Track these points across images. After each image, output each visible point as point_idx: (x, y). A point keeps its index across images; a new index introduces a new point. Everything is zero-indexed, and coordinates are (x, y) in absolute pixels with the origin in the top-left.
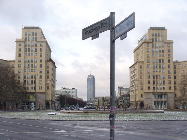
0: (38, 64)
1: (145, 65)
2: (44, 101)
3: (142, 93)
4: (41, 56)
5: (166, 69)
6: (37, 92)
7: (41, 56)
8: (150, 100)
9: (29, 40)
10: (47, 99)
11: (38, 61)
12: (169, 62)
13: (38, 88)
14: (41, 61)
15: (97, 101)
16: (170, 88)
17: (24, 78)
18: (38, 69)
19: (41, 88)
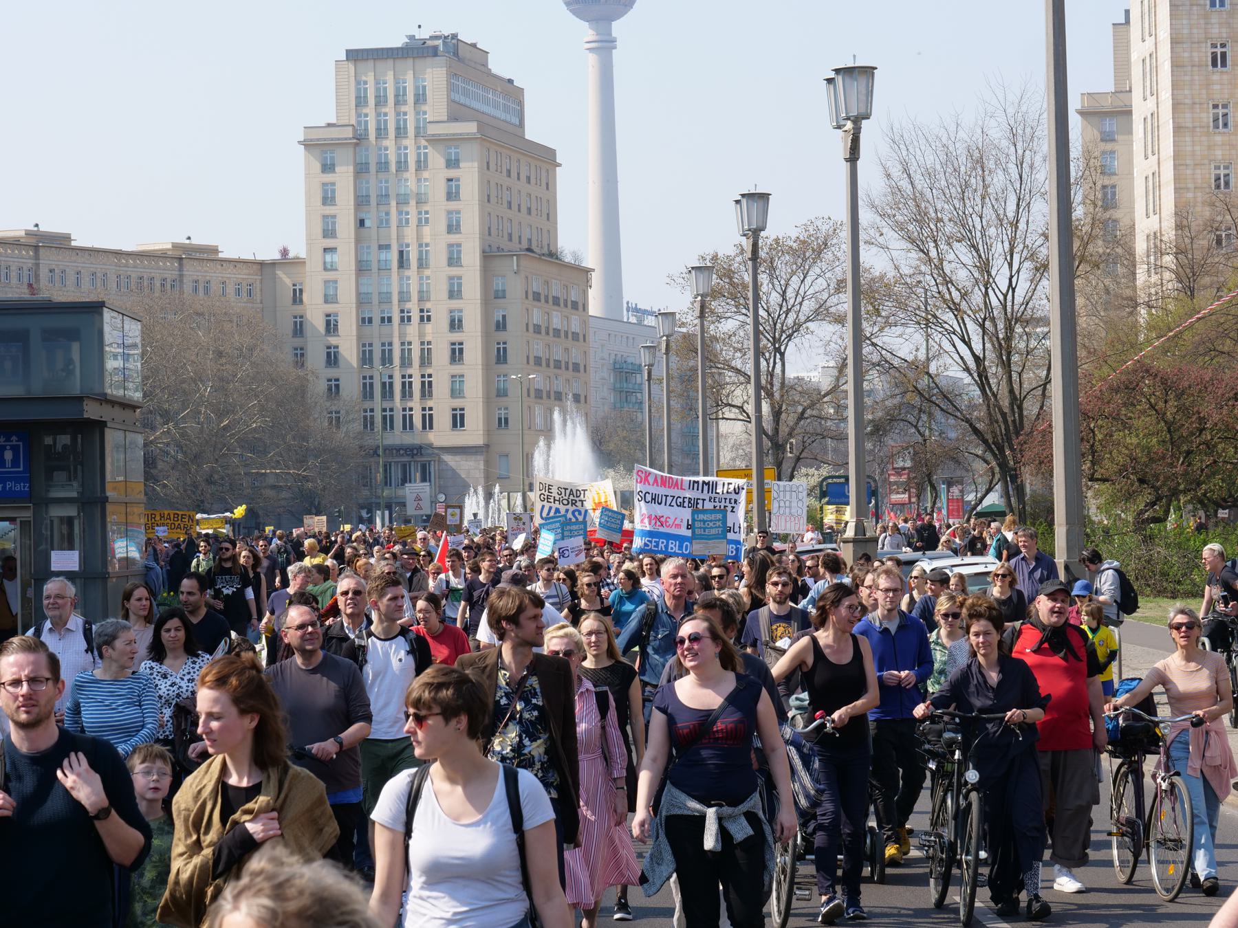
9: (381, 132)
11: (438, 257)
13: (442, 419)
14: (454, 259)
19: (458, 420)
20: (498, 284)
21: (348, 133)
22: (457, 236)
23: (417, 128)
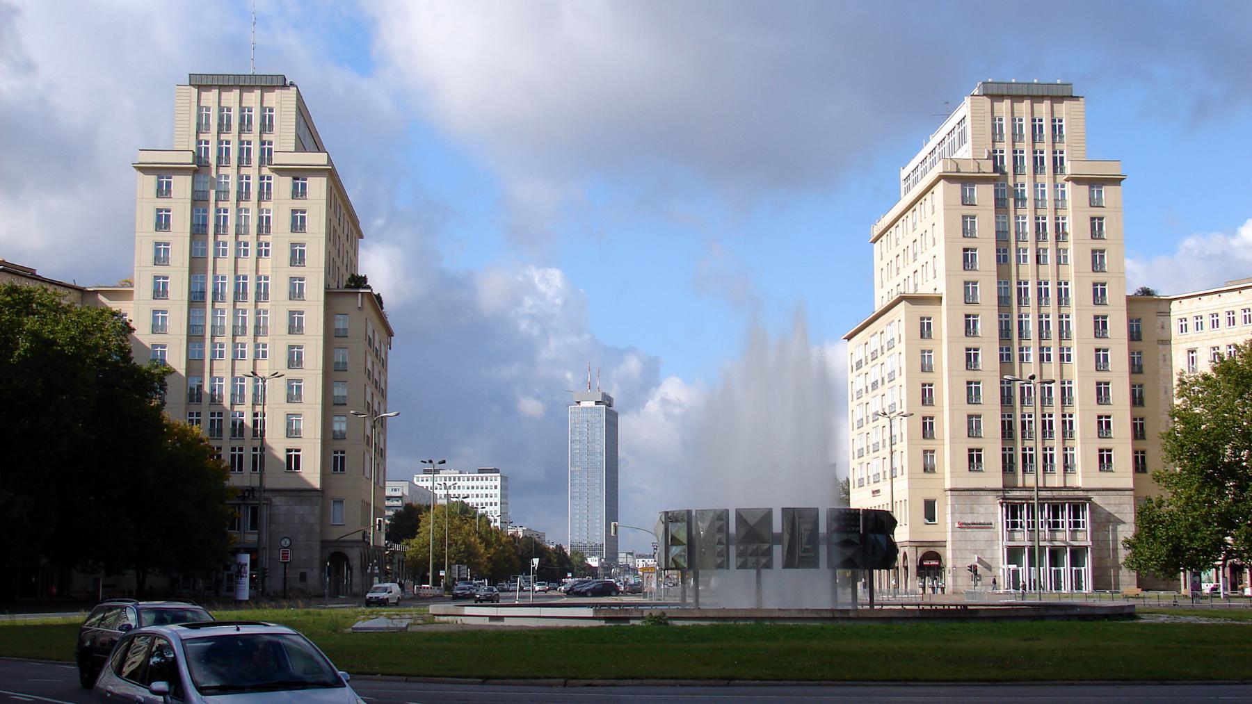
0: (277, 309)
1: (944, 321)
2: (317, 546)
3: (930, 496)
4: (297, 257)
5: (1080, 343)
6: (269, 484)
7: (297, 257)
8: (982, 534)
9: (223, 158)
10: (335, 535)
12: (1099, 293)
14: (296, 291)
15: (683, 536)
16: (1105, 460)
17: (192, 401)
18: (277, 341)
20: (340, 323)
21: (188, 158)
22: (301, 269)
23: (262, 159)
